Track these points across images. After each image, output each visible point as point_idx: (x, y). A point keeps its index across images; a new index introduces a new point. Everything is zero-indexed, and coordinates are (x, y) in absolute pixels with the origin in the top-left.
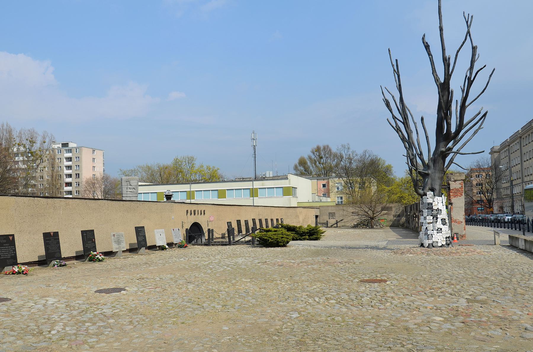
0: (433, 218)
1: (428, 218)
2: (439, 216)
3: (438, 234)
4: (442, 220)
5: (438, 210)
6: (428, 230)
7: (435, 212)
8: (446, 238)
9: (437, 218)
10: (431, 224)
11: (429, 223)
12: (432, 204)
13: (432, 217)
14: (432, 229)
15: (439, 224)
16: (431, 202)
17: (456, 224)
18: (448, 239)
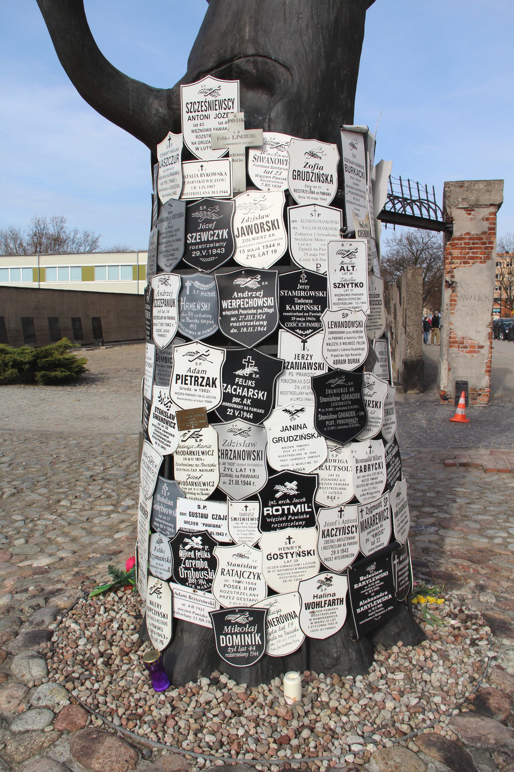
1: (181, 362)
2: (288, 346)
3: (274, 540)
4: (319, 385)
6: (176, 494)
9: (271, 370)
10: (209, 433)
11: (188, 420)
13: (217, 357)
14: (212, 478)
15: (290, 435)
16: (219, 189)
17: (462, 353)
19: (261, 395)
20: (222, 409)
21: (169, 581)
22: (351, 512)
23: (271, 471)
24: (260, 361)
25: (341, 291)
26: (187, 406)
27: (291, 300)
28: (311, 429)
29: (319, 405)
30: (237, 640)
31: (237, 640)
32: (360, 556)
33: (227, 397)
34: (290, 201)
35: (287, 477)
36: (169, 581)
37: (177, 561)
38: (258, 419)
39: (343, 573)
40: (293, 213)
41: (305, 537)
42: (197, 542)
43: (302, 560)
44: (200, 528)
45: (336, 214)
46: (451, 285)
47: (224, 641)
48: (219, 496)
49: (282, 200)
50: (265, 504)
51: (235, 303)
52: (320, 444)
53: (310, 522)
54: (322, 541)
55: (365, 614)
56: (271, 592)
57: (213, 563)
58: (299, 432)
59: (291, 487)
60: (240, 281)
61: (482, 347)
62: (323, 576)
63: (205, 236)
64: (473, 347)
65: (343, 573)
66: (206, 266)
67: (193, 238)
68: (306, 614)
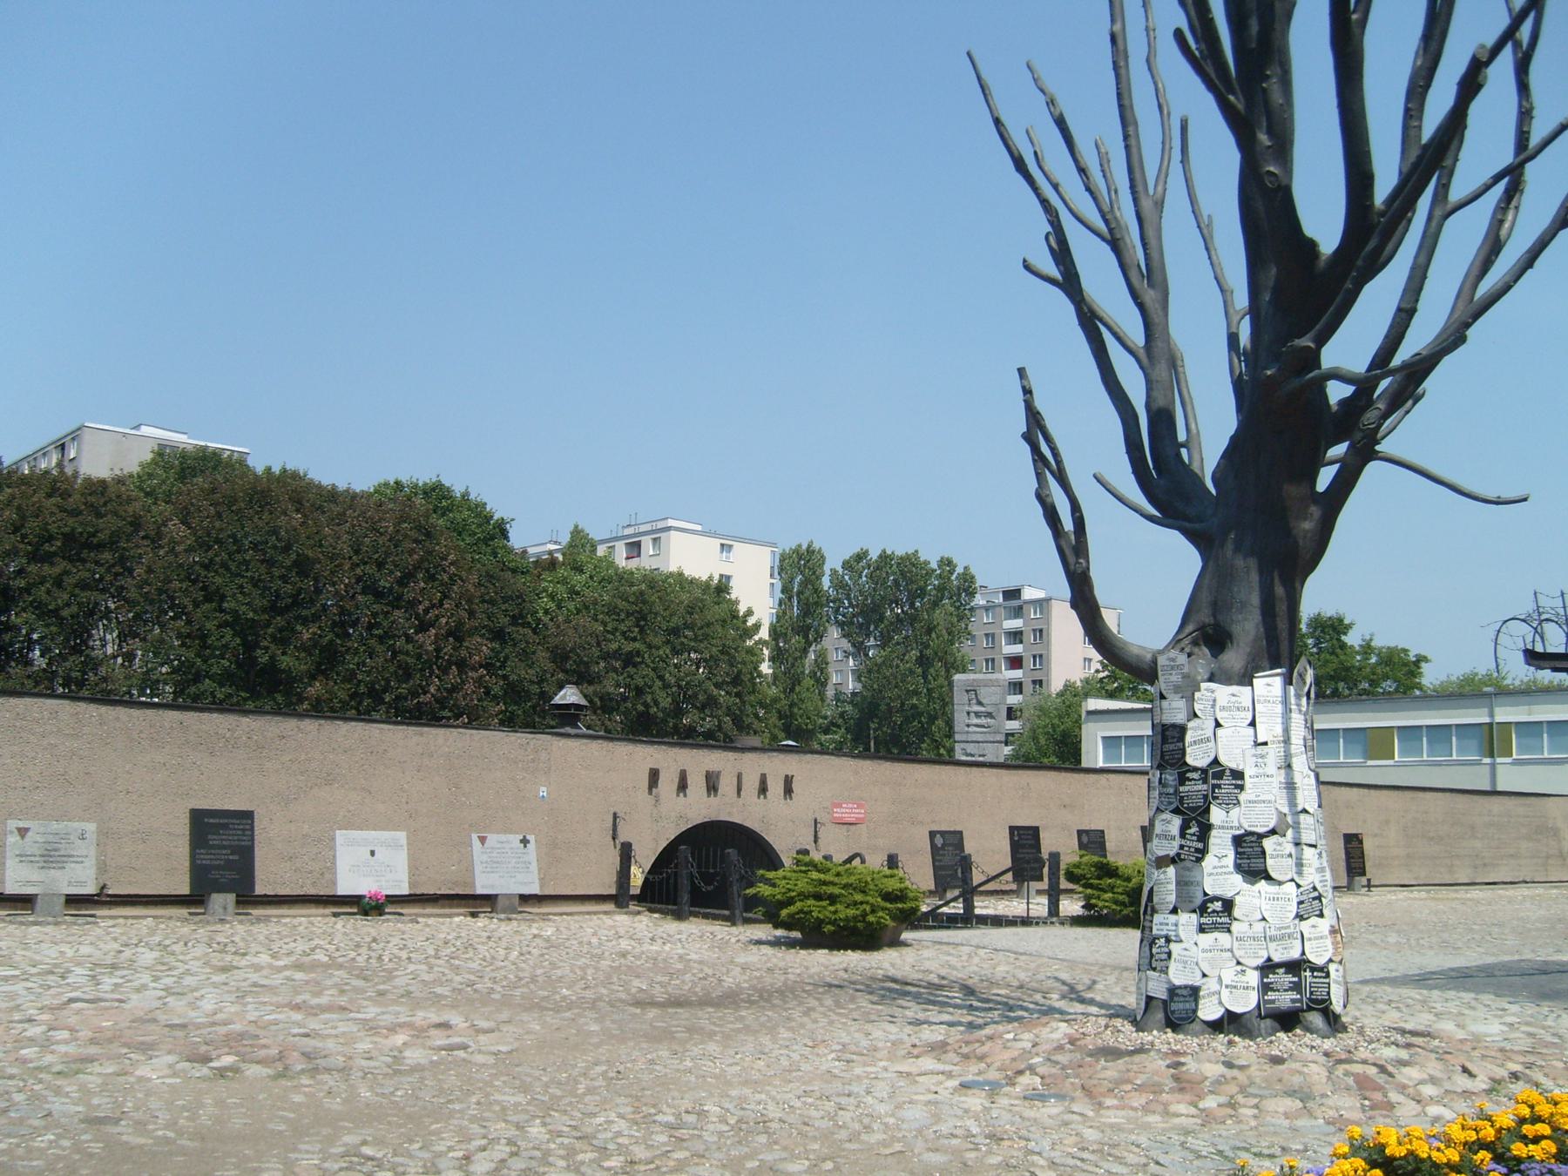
2: (1216, 815)
3: (1206, 939)
4: (1238, 841)
5: (1215, 770)
8: (1268, 967)
9: (1206, 829)
10: (1171, 870)
12: (1181, 730)
13: (1177, 822)
16: (1180, 718)
18: (1282, 978)
19: (1200, 846)
20: (1178, 855)
22: (1259, 927)
23: (1206, 894)
24: (1200, 824)
26: (1161, 853)
27: (1219, 787)
28: (1231, 869)
29: (1237, 853)
30: (1181, 1006)
31: (1181, 1006)
32: (1269, 959)
33: (1182, 847)
34: (1218, 725)
35: (1216, 899)
37: (1152, 955)
38: (1199, 860)
39: (1256, 968)
40: (1220, 732)
45: (1251, 730)
47: (1174, 1006)
48: (1174, 911)
49: (1213, 724)
52: (1238, 879)
55: (1273, 1002)
56: (1204, 975)
57: (1169, 954)
59: (1218, 905)
60: (1189, 775)
62: (1239, 968)
65: (1256, 968)
66: (1172, 765)
67: (1167, 747)
68: (1225, 993)
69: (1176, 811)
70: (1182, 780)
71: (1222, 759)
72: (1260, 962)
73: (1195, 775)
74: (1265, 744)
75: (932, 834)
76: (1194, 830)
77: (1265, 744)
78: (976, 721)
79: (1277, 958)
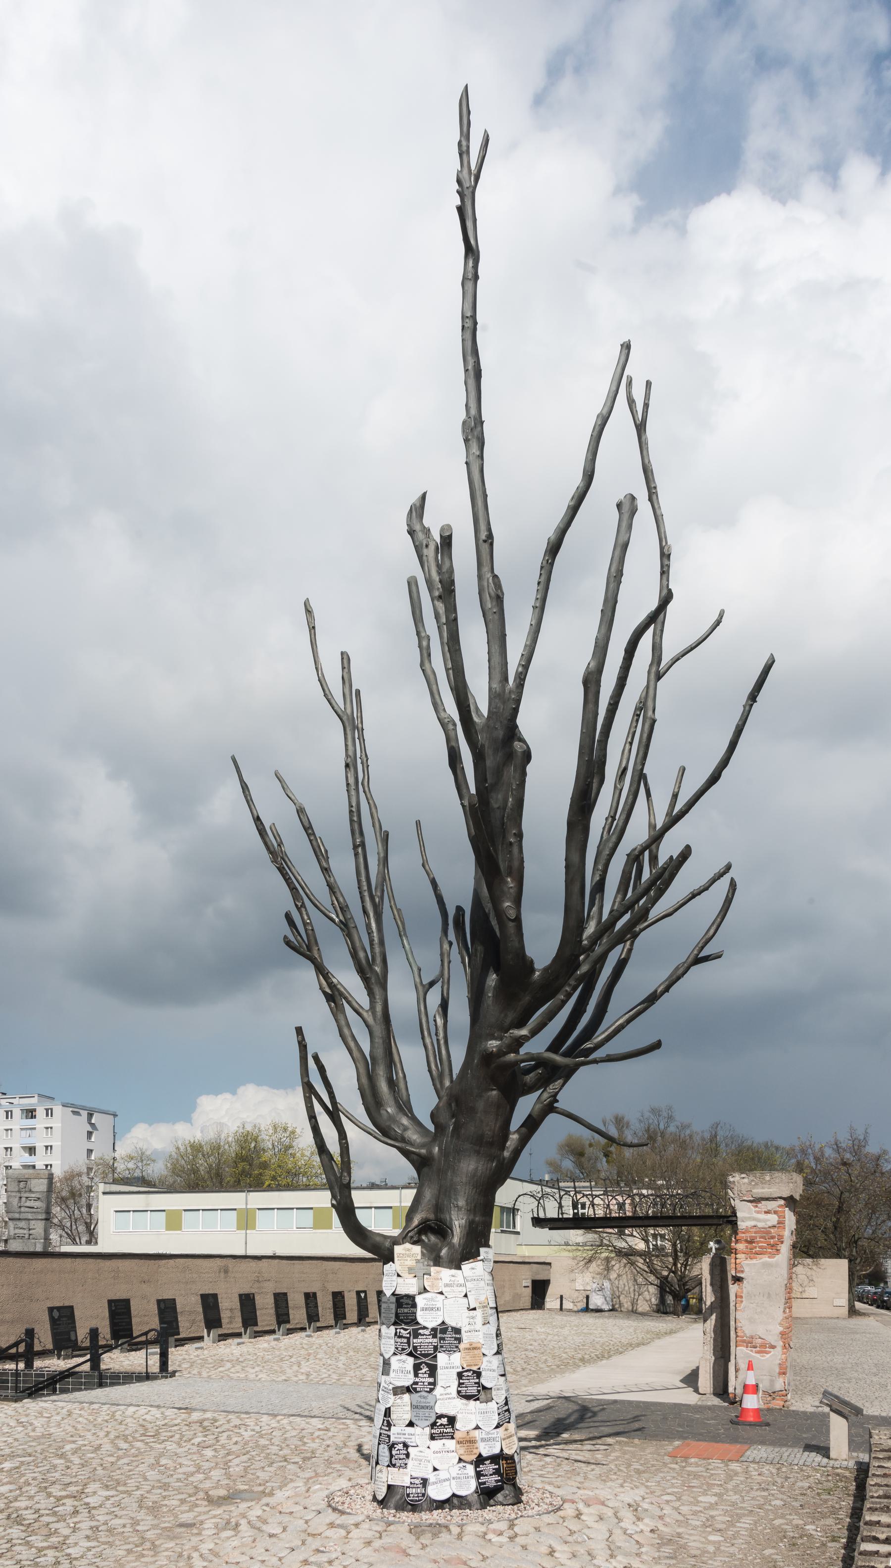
0: (417, 1368)
2: (442, 1359)
3: (437, 1444)
7: (425, 1342)
10: (406, 1397)
11: (398, 1391)
19: (431, 1380)
21: (388, 1466)
25: (469, 1334)
27: (443, 1339)
36: (388, 1466)
37: (391, 1456)
41: (451, 1444)
42: (401, 1446)
43: (450, 1454)
44: (402, 1440)
45: (465, 1299)
46: (738, 1279)
48: (411, 1424)
50: (432, 1428)
51: (419, 1341)
53: (453, 1438)
54: (458, 1446)
56: (435, 1469)
57: (408, 1455)
58: (448, 1396)
59: (444, 1421)
60: (421, 1331)
61: (773, 1347)
63: (406, 1310)
64: (763, 1346)
65: (471, 1463)
67: (400, 1311)
69: (410, 1354)
70: (416, 1335)
71: (447, 1321)
72: (474, 1458)
73: (427, 1332)
74: (474, 1309)
75: (51, 1310)
76: (425, 1369)
77: (474, 1309)
78: (28, 1204)
79: (485, 1454)
